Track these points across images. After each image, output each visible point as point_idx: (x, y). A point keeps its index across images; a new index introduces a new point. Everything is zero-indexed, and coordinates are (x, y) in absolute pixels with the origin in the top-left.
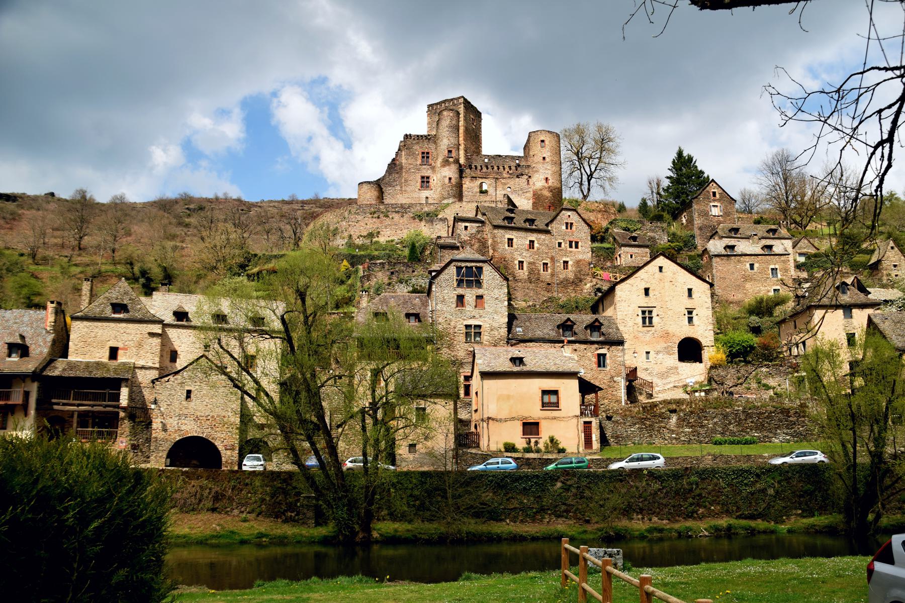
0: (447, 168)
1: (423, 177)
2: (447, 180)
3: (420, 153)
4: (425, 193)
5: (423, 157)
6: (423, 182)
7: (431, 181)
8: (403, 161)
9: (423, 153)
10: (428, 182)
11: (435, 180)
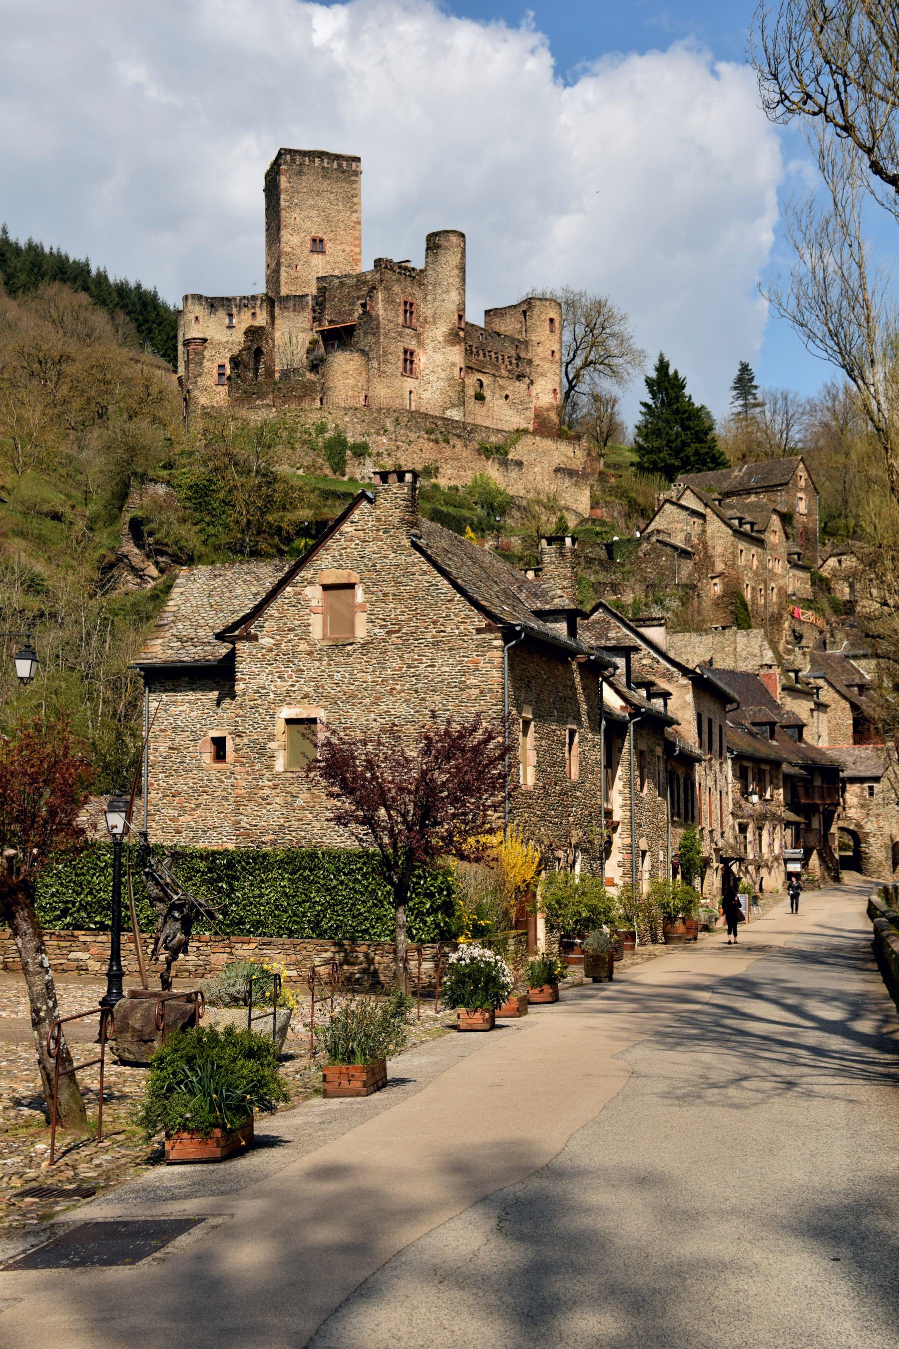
1: (405, 352)
3: (402, 304)
4: (409, 384)
5: (406, 311)
6: (405, 360)
7: (416, 360)
8: (381, 312)
9: (406, 303)
10: (412, 362)
11: (422, 360)
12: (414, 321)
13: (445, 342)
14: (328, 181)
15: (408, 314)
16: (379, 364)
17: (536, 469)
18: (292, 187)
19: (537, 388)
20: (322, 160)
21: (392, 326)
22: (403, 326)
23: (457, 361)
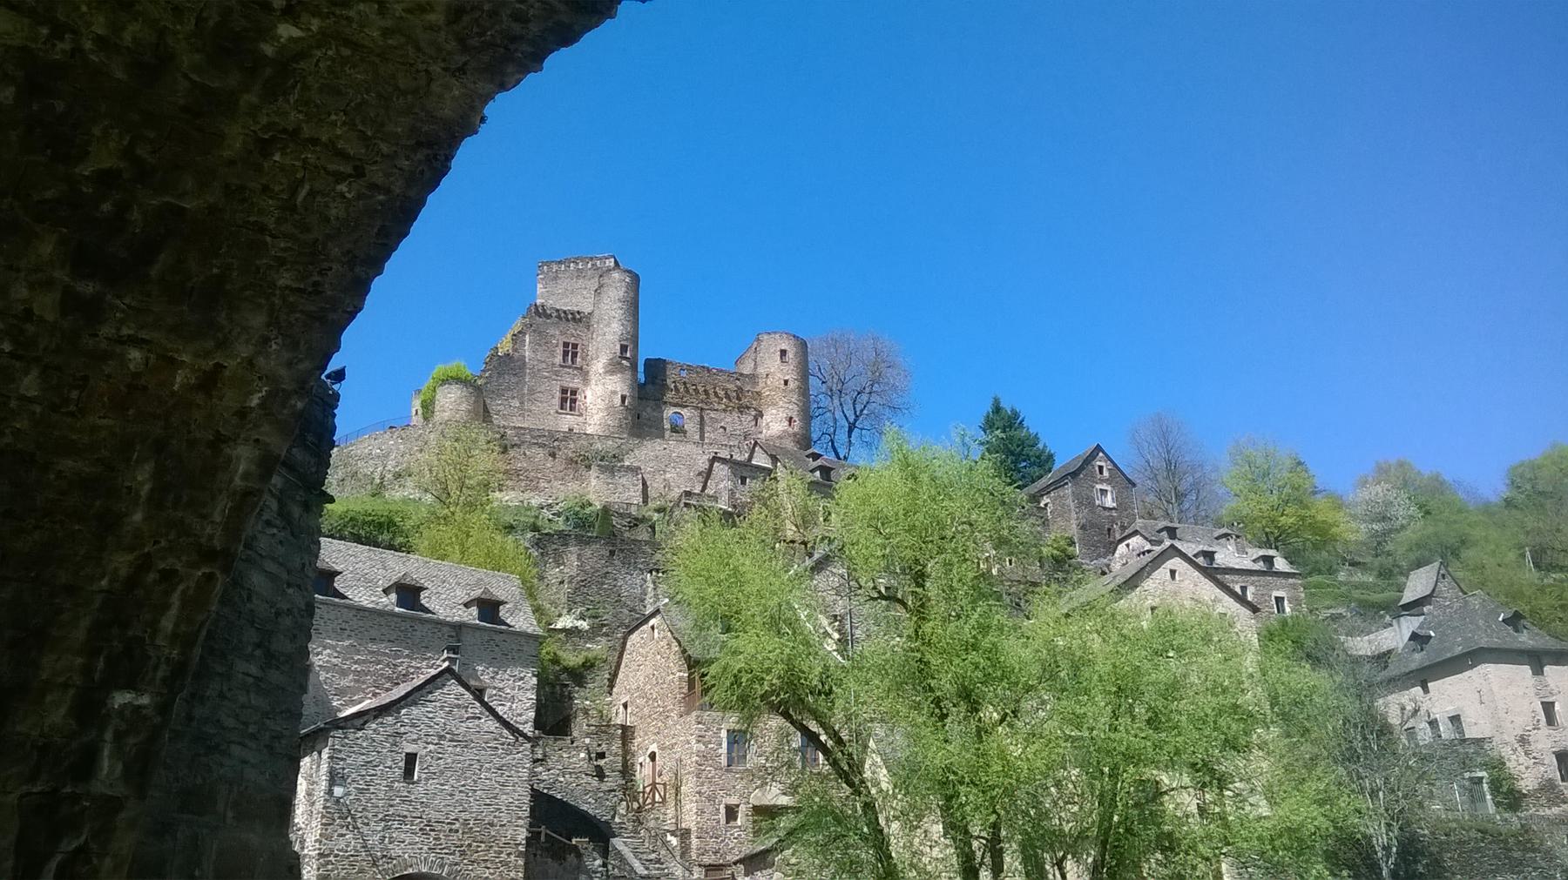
0: (617, 378)
1: (564, 391)
2: (618, 401)
5: (565, 354)
6: (564, 400)
9: (566, 345)
10: (574, 401)
12: (578, 360)
13: (606, 372)
14: (582, 280)
15: (570, 354)
16: (522, 403)
17: (668, 476)
18: (547, 292)
19: (767, 418)
20: (577, 264)
21: (544, 366)
22: (561, 366)
23: (618, 389)
